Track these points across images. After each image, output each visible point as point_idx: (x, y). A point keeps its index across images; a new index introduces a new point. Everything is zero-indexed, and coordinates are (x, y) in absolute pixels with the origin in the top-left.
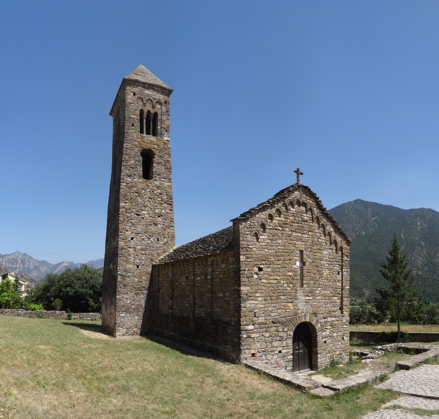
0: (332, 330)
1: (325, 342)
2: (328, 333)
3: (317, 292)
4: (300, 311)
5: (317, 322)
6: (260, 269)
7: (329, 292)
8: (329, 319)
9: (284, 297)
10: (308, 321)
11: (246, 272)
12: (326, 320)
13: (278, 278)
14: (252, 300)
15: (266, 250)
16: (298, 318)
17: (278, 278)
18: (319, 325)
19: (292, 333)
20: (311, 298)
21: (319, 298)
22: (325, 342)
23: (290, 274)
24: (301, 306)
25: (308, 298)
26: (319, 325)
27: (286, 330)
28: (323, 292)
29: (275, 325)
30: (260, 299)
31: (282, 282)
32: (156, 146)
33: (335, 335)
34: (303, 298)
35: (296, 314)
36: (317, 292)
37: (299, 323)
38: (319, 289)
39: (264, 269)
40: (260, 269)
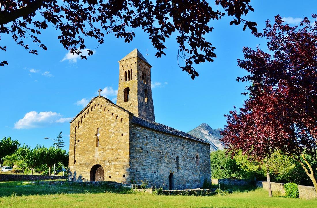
0: (115, 170)
1: (110, 177)
2: (112, 171)
3: (107, 148)
4: (96, 159)
5: (105, 165)
6: (78, 141)
7: (115, 147)
8: (113, 163)
9: (87, 153)
10: (99, 164)
11: (72, 144)
12: (110, 163)
13: (86, 144)
14: (73, 155)
15: (81, 132)
16: (93, 163)
17: (86, 144)
18: (106, 166)
19: (90, 170)
20: (102, 152)
21: (108, 151)
22: (110, 177)
23: (91, 141)
24: (96, 156)
25: (101, 152)
26: (106, 166)
27: (87, 168)
28: (110, 148)
29: (82, 166)
30: (78, 154)
31: (88, 145)
32: (130, 85)
33: (117, 173)
34: (97, 152)
35: (94, 160)
36: (107, 148)
37: (94, 165)
38: (108, 146)
39: (80, 141)
40: (78, 141)
